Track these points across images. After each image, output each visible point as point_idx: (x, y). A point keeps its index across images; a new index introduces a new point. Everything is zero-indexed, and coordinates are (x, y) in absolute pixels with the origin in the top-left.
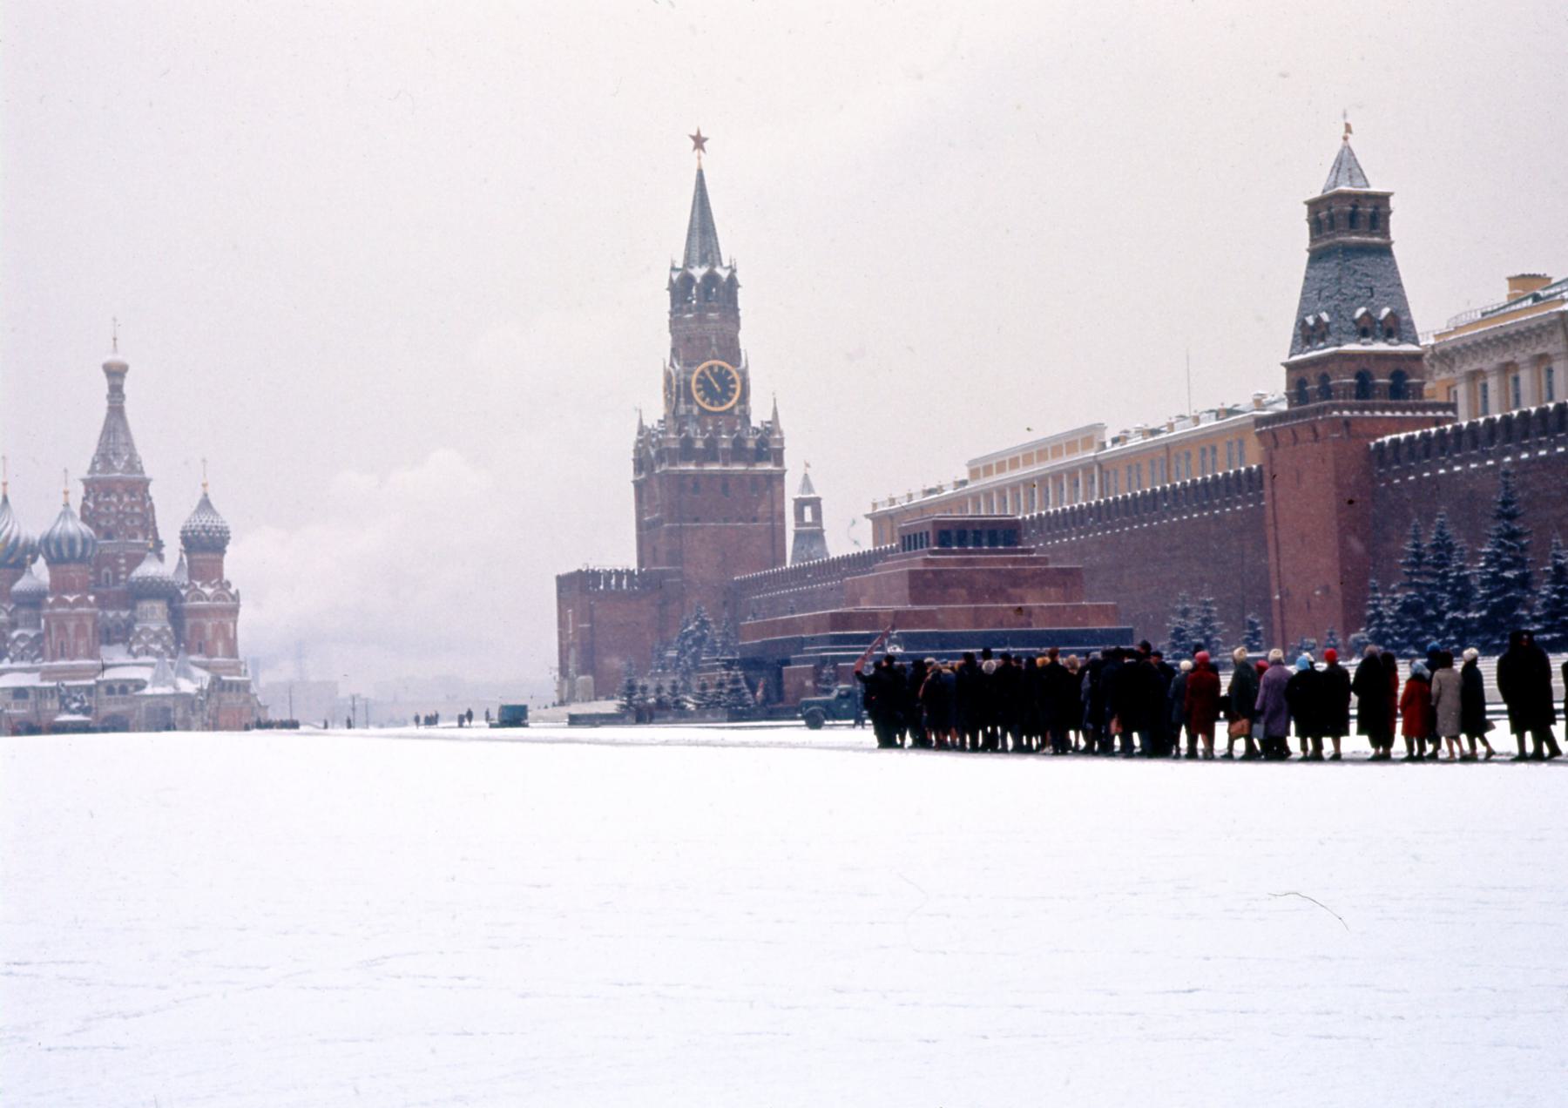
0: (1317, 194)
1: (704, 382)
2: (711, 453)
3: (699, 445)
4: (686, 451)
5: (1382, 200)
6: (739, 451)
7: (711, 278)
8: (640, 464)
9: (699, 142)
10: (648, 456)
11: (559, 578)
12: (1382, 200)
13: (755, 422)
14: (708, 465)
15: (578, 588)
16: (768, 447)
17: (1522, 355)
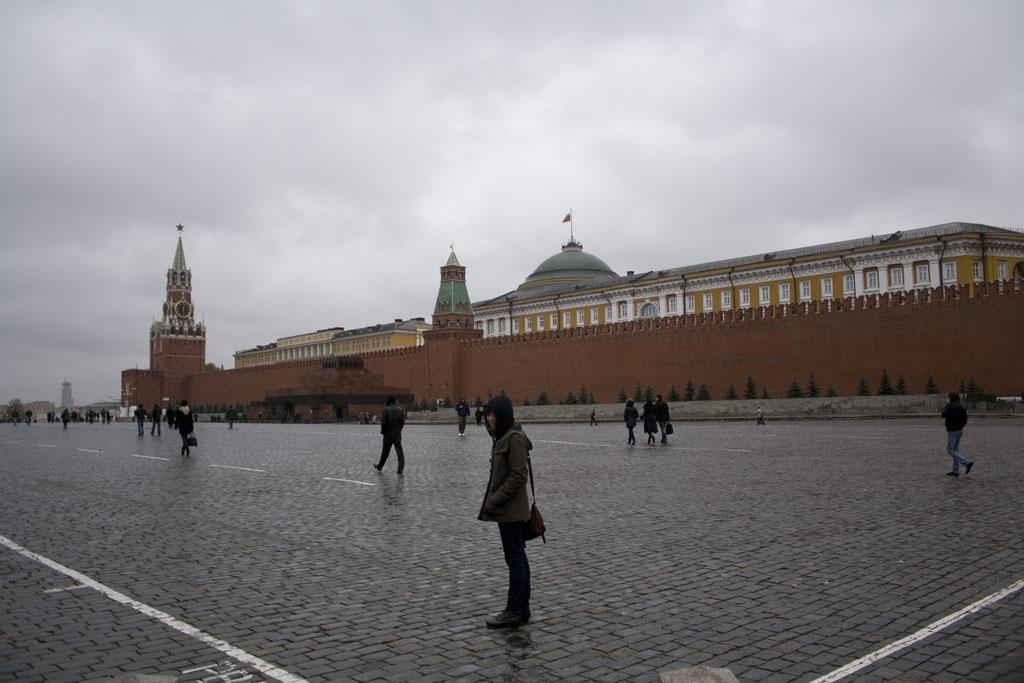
0: (444, 264)
1: (180, 307)
2: (181, 332)
3: (177, 329)
4: (173, 331)
5: (463, 268)
6: (191, 332)
7: (183, 274)
8: (153, 334)
9: (180, 228)
10: (155, 333)
11: (123, 372)
12: (463, 268)
13: (197, 322)
14: (178, 338)
15: (130, 376)
16: (200, 331)
17: (495, 317)
